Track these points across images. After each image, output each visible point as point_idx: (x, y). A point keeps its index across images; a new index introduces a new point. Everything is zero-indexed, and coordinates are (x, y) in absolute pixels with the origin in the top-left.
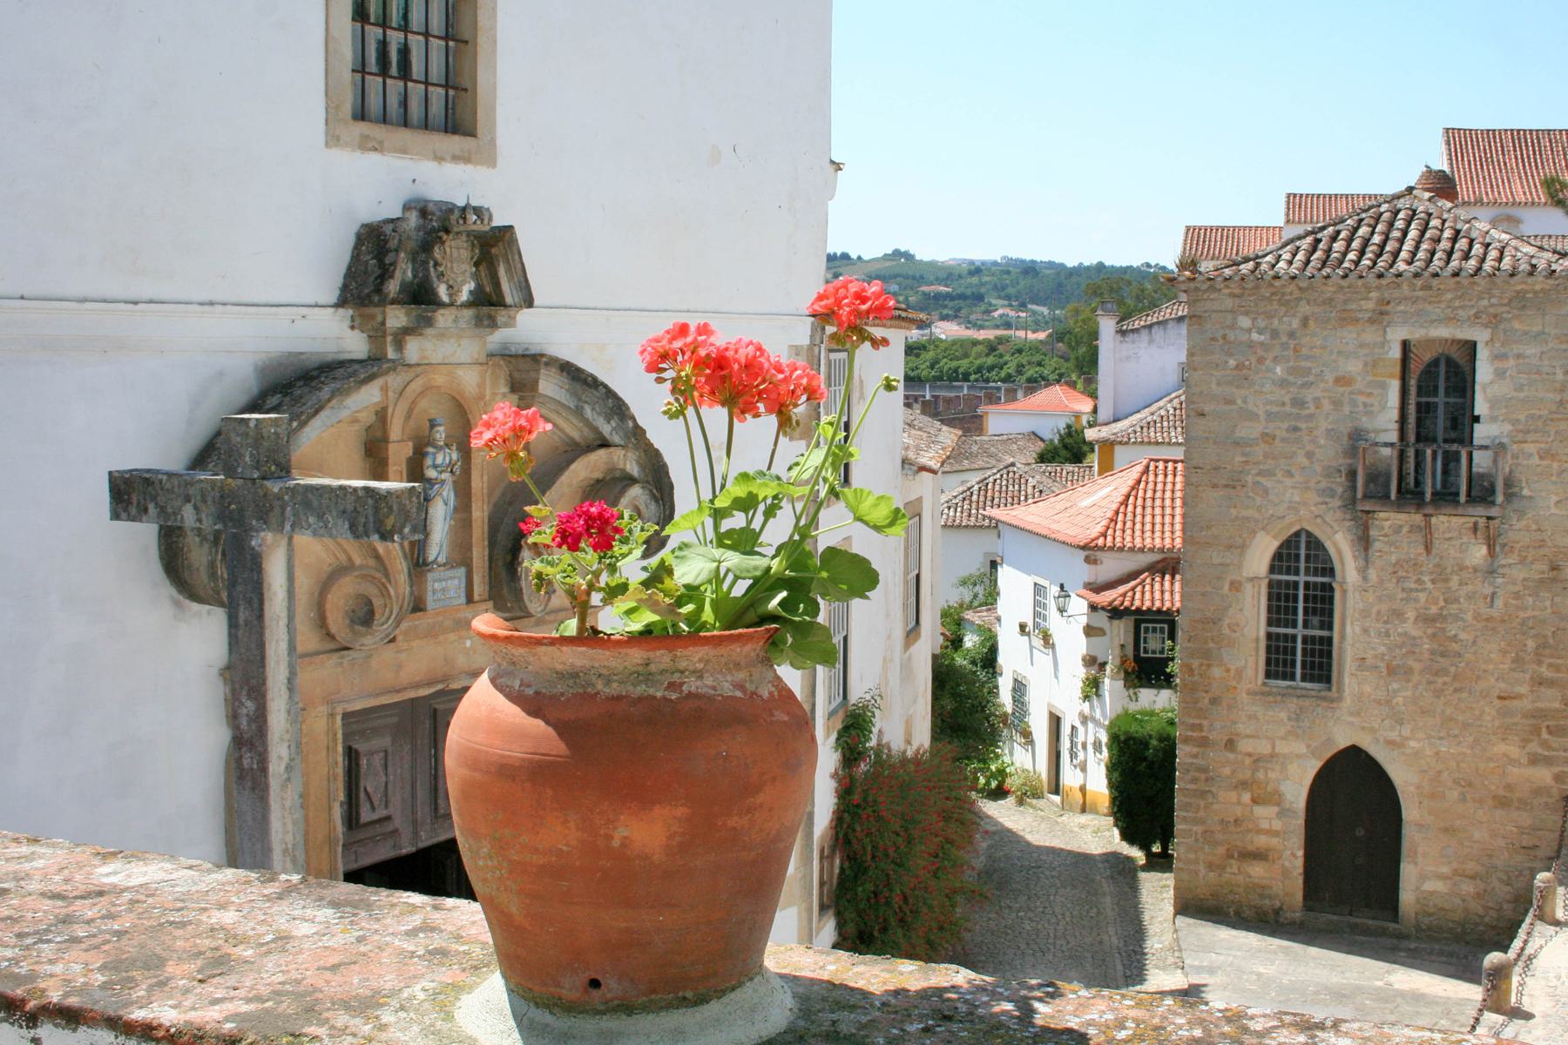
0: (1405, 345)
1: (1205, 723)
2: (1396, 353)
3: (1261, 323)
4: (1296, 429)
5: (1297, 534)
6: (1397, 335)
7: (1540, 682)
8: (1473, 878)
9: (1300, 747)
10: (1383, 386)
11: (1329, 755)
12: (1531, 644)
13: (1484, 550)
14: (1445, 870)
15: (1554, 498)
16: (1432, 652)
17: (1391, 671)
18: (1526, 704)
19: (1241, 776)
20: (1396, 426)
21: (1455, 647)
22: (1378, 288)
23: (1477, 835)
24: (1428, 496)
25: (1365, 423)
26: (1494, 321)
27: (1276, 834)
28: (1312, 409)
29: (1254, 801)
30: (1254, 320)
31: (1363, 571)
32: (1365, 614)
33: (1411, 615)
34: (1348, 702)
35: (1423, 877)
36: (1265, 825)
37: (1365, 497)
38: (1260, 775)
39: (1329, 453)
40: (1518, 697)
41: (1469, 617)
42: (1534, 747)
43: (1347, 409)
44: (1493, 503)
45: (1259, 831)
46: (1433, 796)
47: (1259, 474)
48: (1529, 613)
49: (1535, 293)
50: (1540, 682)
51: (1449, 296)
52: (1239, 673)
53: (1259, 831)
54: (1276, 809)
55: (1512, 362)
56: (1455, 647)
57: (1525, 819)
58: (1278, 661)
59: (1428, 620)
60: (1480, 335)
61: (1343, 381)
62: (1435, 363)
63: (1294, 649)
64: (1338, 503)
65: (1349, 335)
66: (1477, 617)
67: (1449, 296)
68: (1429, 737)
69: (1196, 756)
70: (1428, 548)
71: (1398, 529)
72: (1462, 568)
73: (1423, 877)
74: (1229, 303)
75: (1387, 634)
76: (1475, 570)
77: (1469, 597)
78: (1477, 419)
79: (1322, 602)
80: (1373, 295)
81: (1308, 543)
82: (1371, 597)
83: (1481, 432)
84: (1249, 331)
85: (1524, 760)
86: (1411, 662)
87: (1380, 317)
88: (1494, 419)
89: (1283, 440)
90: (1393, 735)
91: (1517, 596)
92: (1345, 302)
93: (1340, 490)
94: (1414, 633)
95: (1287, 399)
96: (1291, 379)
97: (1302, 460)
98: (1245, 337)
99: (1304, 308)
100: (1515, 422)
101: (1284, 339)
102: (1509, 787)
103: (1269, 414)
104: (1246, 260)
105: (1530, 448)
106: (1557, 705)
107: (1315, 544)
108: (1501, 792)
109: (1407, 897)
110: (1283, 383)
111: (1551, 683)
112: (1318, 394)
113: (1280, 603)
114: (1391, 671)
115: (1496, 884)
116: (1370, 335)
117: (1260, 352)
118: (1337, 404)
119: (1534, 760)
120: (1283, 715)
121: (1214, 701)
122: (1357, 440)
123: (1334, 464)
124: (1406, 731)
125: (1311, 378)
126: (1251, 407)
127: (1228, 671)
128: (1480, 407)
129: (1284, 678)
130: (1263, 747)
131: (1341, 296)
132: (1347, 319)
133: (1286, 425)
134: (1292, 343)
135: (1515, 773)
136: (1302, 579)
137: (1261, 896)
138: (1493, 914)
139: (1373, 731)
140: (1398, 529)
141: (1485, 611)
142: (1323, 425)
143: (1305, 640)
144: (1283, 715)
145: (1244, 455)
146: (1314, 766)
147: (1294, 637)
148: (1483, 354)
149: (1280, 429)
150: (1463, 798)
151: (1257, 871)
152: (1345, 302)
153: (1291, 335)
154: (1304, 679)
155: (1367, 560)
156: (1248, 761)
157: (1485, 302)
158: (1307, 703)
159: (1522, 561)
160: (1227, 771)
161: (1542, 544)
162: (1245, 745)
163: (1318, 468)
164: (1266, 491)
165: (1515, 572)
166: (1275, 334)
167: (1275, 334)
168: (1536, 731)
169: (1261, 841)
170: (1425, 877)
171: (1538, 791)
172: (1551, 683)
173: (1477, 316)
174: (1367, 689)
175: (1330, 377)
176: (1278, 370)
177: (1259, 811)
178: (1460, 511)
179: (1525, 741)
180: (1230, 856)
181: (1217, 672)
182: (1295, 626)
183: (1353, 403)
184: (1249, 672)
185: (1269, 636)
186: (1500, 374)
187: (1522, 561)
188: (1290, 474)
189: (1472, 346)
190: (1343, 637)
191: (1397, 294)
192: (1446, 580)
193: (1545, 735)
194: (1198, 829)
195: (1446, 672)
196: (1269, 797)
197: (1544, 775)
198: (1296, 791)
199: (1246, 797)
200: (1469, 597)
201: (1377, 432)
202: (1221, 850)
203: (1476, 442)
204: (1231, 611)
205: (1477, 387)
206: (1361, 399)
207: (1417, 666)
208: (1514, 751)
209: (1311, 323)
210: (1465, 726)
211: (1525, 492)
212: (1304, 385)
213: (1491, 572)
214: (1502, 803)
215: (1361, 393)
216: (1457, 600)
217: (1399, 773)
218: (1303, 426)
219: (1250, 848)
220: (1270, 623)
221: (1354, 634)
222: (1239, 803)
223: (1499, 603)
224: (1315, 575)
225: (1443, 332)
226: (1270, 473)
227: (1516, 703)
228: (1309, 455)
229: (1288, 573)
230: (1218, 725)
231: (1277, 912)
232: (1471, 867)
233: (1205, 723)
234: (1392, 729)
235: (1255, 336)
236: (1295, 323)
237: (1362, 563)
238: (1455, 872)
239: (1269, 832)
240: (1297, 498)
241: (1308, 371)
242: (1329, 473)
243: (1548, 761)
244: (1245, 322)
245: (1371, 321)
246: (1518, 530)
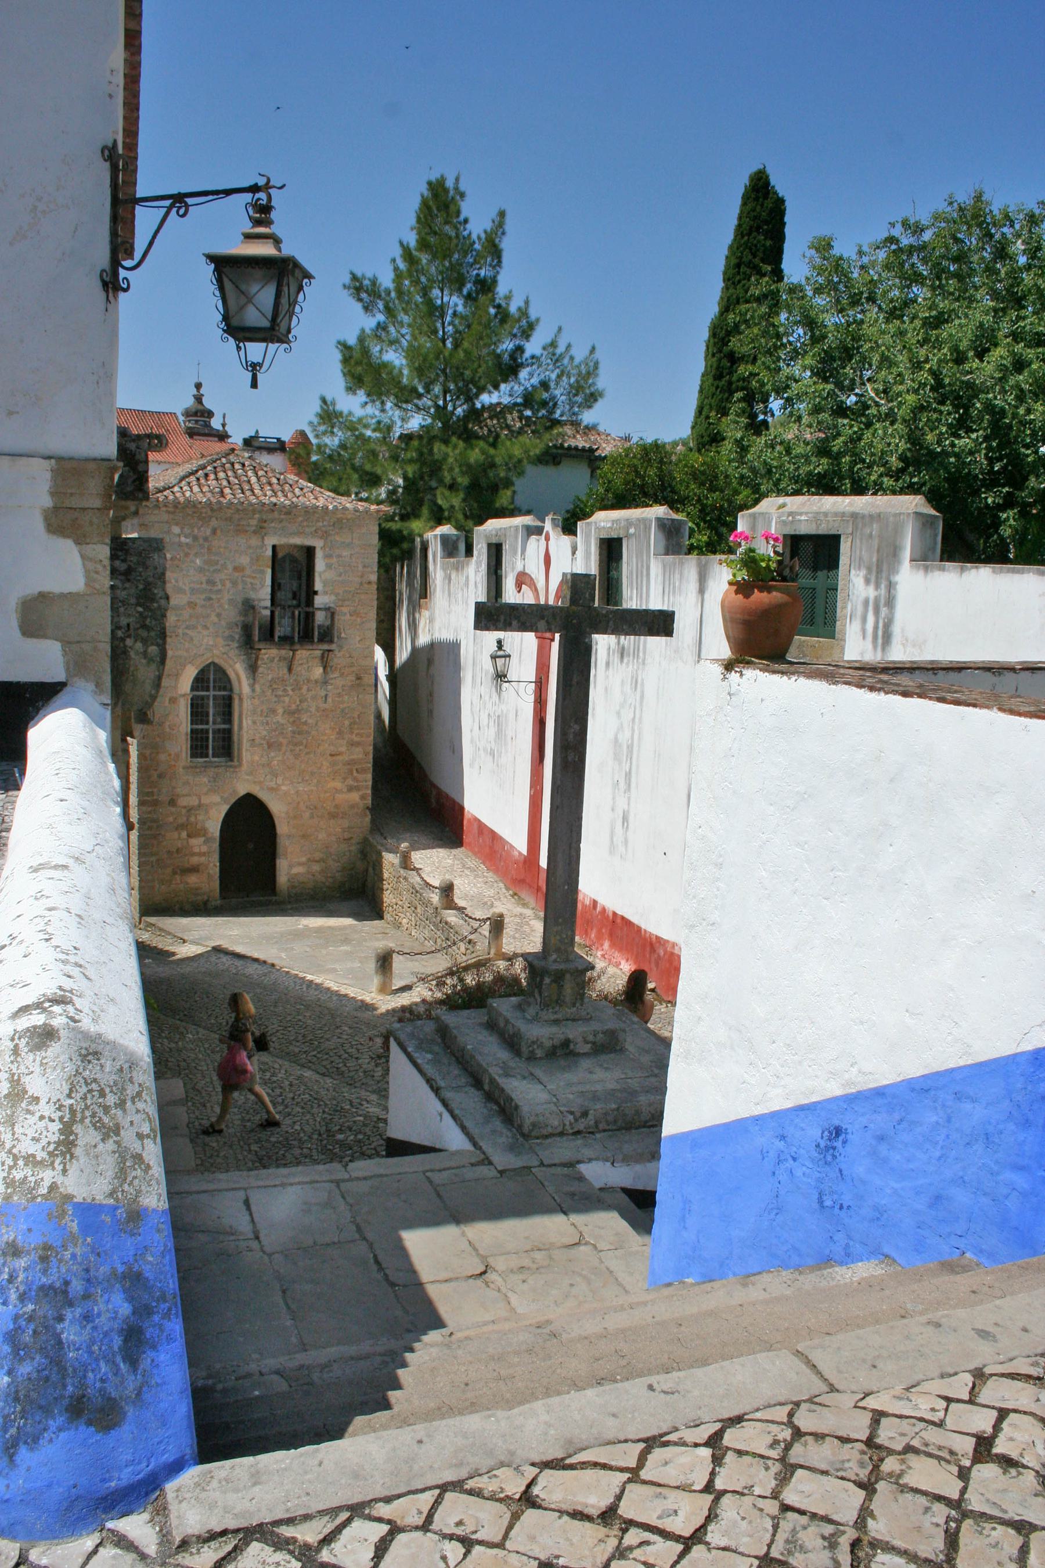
0: (274, 547)
1: (155, 790)
2: (269, 553)
3: (187, 530)
4: (210, 599)
5: (208, 666)
6: (271, 541)
7: (352, 744)
9: (216, 798)
10: (263, 572)
11: (234, 801)
12: (347, 723)
13: (321, 670)
14: (304, 859)
15: (358, 639)
16: (294, 732)
17: (270, 745)
18: (346, 758)
19: (180, 821)
20: (269, 597)
22: (260, 512)
23: (320, 837)
24: (296, 639)
25: (252, 595)
26: (325, 535)
27: (204, 854)
28: (220, 587)
29: (189, 836)
30: (182, 529)
31: (252, 686)
32: (254, 712)
33: (280, 711)
34: (245, 767)
35: (291, 866)
37: (260, 640)
38: (192, 819)
39: (232, 614)
41: (313, 709)
43: (240, 587)
44: (331, 641)
45: (194, 854)
46: (295, 817)
47: (187, 628)
48: (345, 705)
49: (348, 520)
51: (301, 519)
52: (177, 755)
53: (194, 854)
54: (203, 839)
57: (346, 823)
59: (292, 713)
60: (317, 543)
62: (284, 557)
63: (207, 738)
65: (242, 540)
66: (318, 709)
67: (301, 519)
68: (292, 783)
69: (150, 812)
70: (290, 670)
72: (309, 681)
73: (291, 866)
74: (165, 517)
75: (267, 724)
76: (316, 682)
77: (314, 698)
78: (316, 593)
80: (257, 516)
81: (215, 671)
82: (256, 702)
83: (319, 601)
84: (179, 535)
85: (345, 790)
86: (281, 739)
87: (261, 530)
88: (325, 593)
89: (203, 606)
90: (273, 784)
91: (339, 695)
92: (239, 520)
93: (237, 637)
94: (283, 721)
95: (204, 580)
96: (206, 567)
97: (214, 618)
98: (177, 540)
99: (214, 523)
100: (337, 595)
101: (201, 541)
102: (336, 806)
103: (193, 590)
104: (165, 489)
105: (345, 610)
106: (361, 756)
108: (333, 810)
110: (201, 570)
111: (358, 744)
112: (224, 577)
113: (198, 711)
114: (270, 745)
115: (331, 863)
116: (254, 541)
117: (187, 550)
118: (234, 583)
119: (351, 789)
120: (205, 780)
121: (160, 776)
122: (249, 607)
124: (280, 781)
125: (219, 567)
126: (181, 584)
127: (170, 755)
128: (318, 586)
129: (202, 757)
130: (193, 801)
131: (237, 516)
132: (240, 531)
133: (203, 596)
134: (206, 545)
135: (340, 797)
136: (212, 693)
137: (197, 895)
138: (331, 880)
139: (260, 783)
140: (272, 660)
141: (323, 706)
142: (226, 597)
143: (214, 732)
144: (205, 780)
145: (176, 615)
146: (225, 809)
147: (207, 731)
149: (199, 599)
150: (312, 817)
151: (193, 879)
152: (239, 520)
153: (206, 539)
154: (213, 756)
155: (254, 679)
156: (184, 811)
157: (321, 524)
158: (221, 770)
159: (342, 675)
160: (171, 819)
161: (352, 665)
162: (183, 802)
163: (223, 623)
164: (192, 639)
165: (338, 682)
166: (195, 538)
168: (351, 772)
169: (195, 860)
170: (292, 866)
171: (352, 807)
172: (358, 744)
173: (316, 531)
174: (256, 758)
175: (230, 567)
176: (198, 561)
177: (194, 841)
178: (315, 647)
179: (345, 779)
180: (174, 873)
181: (163, 757)
182: (207, 723)
184: (184, 754)
185: (192, 730)
186: (329, 566)
187: (342, 675)
188: (206, 627)
190: (240, 728)
191: (270, 516)
192: (300, 689)
193: (355, 774)
194: (153, 859)
195: (301, 743)
196: (202, 832)
197: (355, 796)
198: (214, 825)
199: (184, 834)
200: (314, 698)
201: (260, 600)
202: (169, 870)
203: (316, 606)
204: (170, 718)
205: (317, 575)
206: (249, 580)
207: (285, 742)
208: (338, 784)
209: (218, 532)
210: (312, 774)
211: (343, 635)
212: (214, 571)
213: (325, 683)
214: (333, 816)
215: (249, 577)
216: (306, 700)
217: (276, 807)
218: (214, 597)
219: (187, 865)
220: (192, 724)
221: (248, 726)
222: (179, 838)
223: (329, 700)
224: (220, 690)
225: (297, 541)
226: (194, 627)
227: (340, 758)
228: (219, 615)
229: (203, 690)
230: (164, 790)
231: (206, 903)
232: (318, 855)
233: (155, 790)
234: (271, 781)
235: (183, 539)
236: (208, 532)
237: (251, 681)
238: (309, 860)
240: (211, 643)
241: (217, 563)
242: (230, 626)
244: (176, 530)
245: (255, 532)
246: (339, 658)
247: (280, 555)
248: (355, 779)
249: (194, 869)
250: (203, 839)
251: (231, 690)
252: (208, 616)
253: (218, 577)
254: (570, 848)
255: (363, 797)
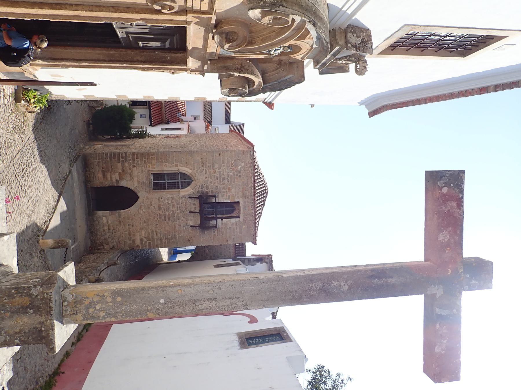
0: (238, 202)
4: (217, 178)
5: (190, 179)
7: (161, 240)
8: (109, 229)
9: (136, 184)
10: (229, 199)
13: (192, 224)
18: (155, 237)
21: (167, 220)
25: (220, 195)
26: (245, 221)
31: (184, 196)
36: (113, 176)
40: (157, 235)
42: (145, 240)
43: (223, 190)
50: (161, 240)
54: (118, 179)
55: (235, 226)
56: (167, 220)
58: (157, 176)
60: (241, 219)
61: (229, 189)
64: (200, 190)
71: (194, 204)
78: (222, 220)
79: (175, 186)
81: (189, 182)
83: (219, 221)
84: (240, 165)
85: (142, 237)
87: (245, 196)
88: (222, 224)
90: (143, 207)
97: (210, 180)
100: (222, 228)
101: (239, 175)
107: (189, 184)
109: (100, 213)
110: (228, 175)
113: (173, 175)
116: (240, 194)
118: (224, 188)
119: (141, 240)
121: (145, 162)
123: (210, 188)
134: (238, 177)
135: (138, 235)
136: (180, 181)
137: (93, 177)
142: (219, 186)
146: (133, 189)
148: (237, 220)
151: (100, 175)
167: (240, 172)
170: (106, 218)
171: (134, 241)
182: (168, 180)
183: (224, 192)
186: (233, 224)
188: (206, 178)
189: (238, 217)
195: (160, 218)
197: (138, 242)
199: (120, 171)
228: (211, 182)
232: (112, 228)
235: (239, 167)
239: (111, 177)
243: (142, 243)
244: (243, 164)
247: (235, 205)
248: (146, 242)
249: (104, 176)
250: (118, 179)
251: (181, 189)
252: (211, 178)
253: (226, 181)
254: (210, 299)
255: (138, 246)
